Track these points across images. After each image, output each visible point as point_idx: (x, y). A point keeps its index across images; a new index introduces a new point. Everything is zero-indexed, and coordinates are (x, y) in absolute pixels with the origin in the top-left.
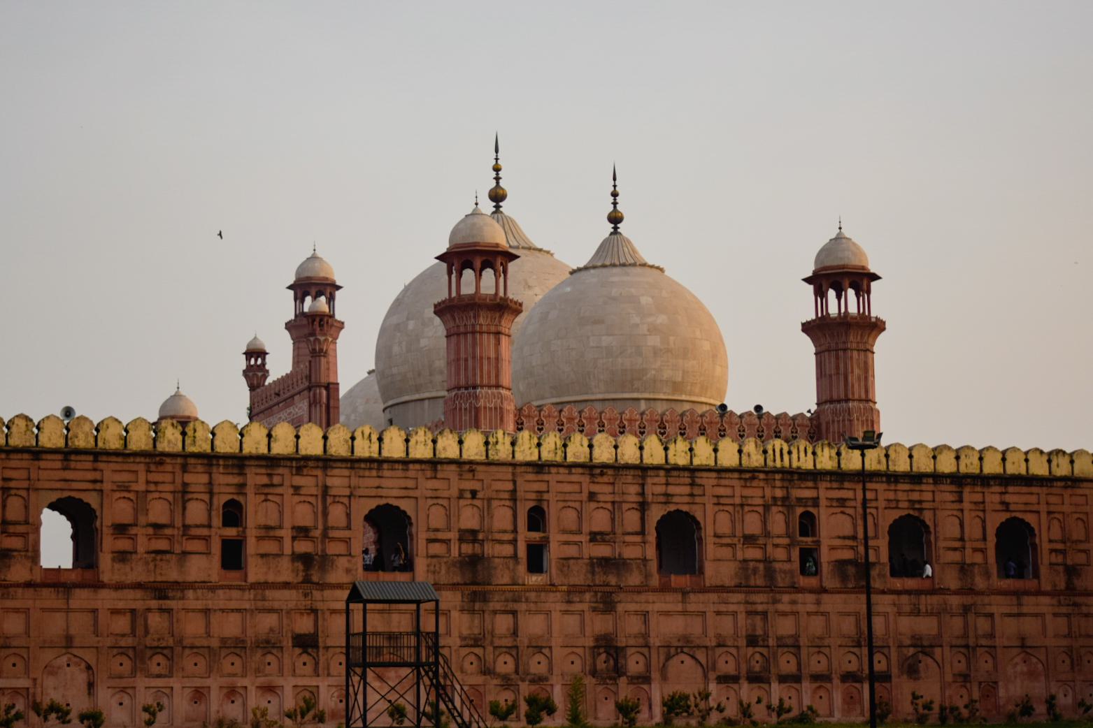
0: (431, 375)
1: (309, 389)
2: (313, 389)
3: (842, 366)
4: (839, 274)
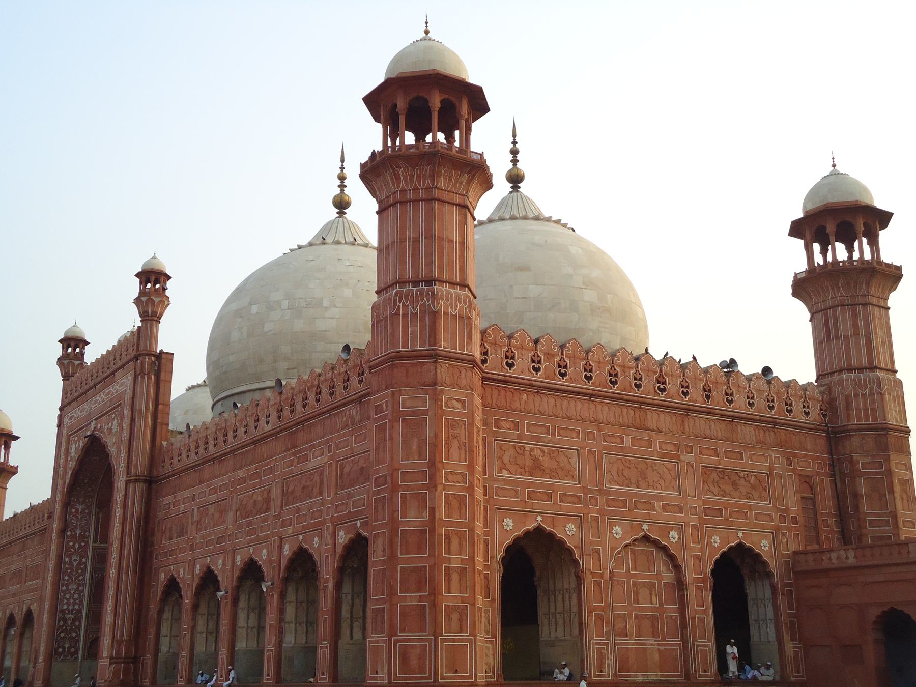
0: (275, 361)
1: (136, 358)
2: (140, 359)
3: (861, 323)
4: (839, 218)
